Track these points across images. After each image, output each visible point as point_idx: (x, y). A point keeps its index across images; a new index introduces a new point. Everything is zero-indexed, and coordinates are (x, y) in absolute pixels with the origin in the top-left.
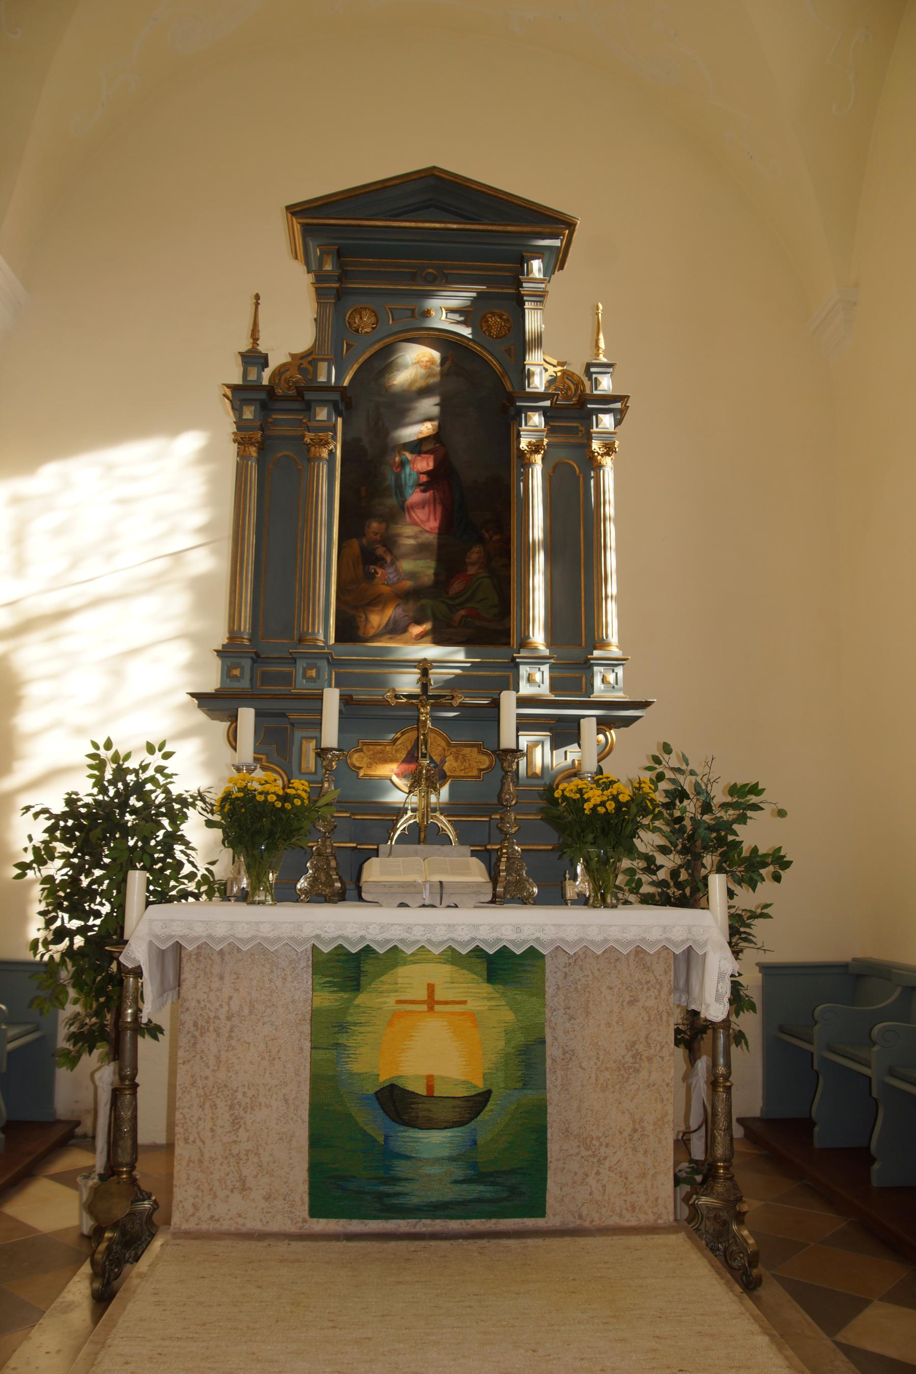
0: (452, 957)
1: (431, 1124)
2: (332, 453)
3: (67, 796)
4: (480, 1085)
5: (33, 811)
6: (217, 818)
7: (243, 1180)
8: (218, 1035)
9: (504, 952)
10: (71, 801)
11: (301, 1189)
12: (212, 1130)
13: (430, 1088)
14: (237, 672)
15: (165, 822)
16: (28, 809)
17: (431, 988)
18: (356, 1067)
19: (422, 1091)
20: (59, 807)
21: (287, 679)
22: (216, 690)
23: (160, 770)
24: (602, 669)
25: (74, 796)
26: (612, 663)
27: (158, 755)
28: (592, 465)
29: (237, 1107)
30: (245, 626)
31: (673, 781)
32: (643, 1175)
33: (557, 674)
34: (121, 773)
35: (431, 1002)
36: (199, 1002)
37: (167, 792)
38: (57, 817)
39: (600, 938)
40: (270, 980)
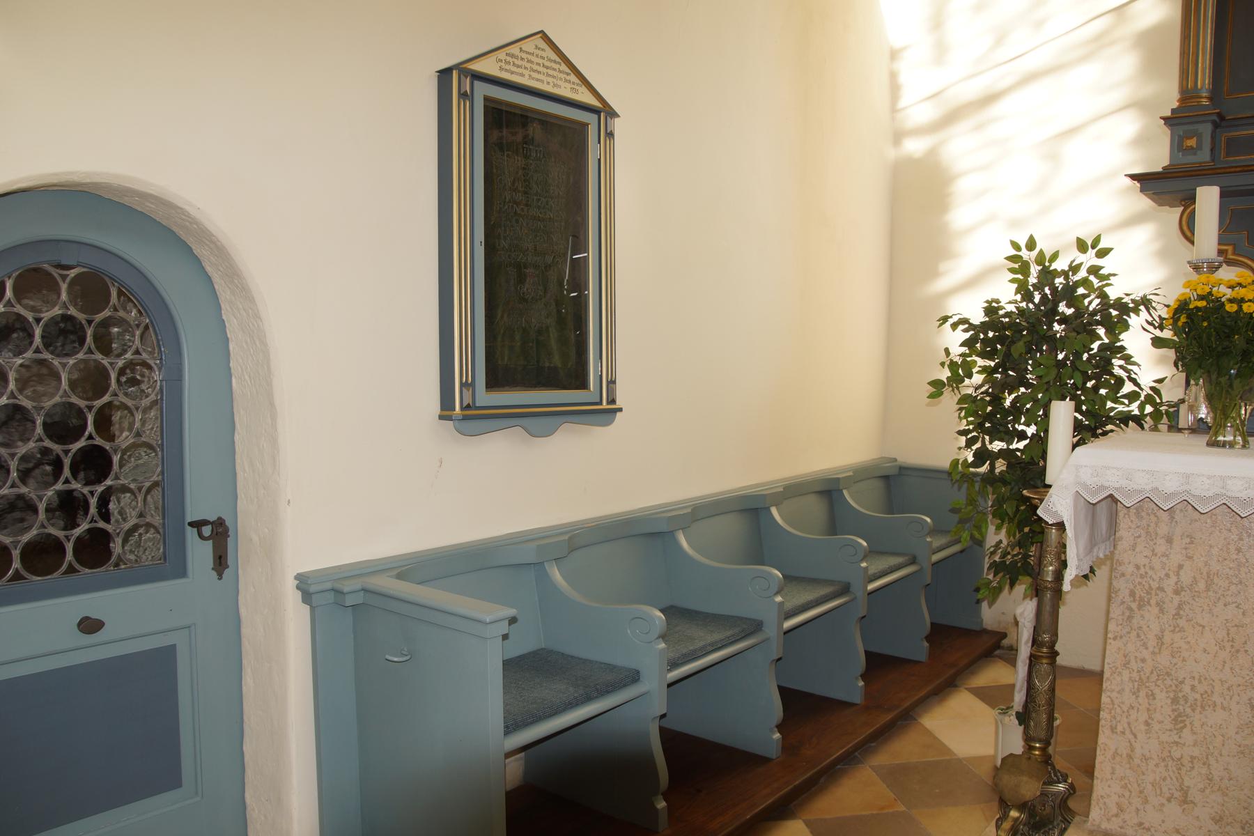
3: (986, 305)
5: (951, 321)
6: (1167, 334)
7: (1185, 791)
8: (1162, 611)
12: (1147, 723)
14: (1192, 142)
15: (1101, 331)
16: (945, 319)
20: (978, 317)
22: (1164, 168)
23: (1094, 270)
25: (994, 304)
27: (1091, 253)
29: (1182, 702)
34: (1047, 275)
36: (1138, 567)
37: (1103, 296)
40: (1239, 550)
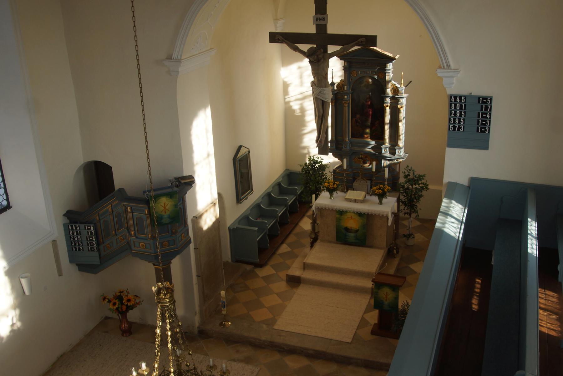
0: (354, 212)
1: (351, 232)
2: (349, 104)
4: (358, 229)
9: (361, 213)
17: (351, 216)
19: (350, 228)
24: (398, 150)
30: (334, 138)
31: (408, 172)
35: (351, 218)
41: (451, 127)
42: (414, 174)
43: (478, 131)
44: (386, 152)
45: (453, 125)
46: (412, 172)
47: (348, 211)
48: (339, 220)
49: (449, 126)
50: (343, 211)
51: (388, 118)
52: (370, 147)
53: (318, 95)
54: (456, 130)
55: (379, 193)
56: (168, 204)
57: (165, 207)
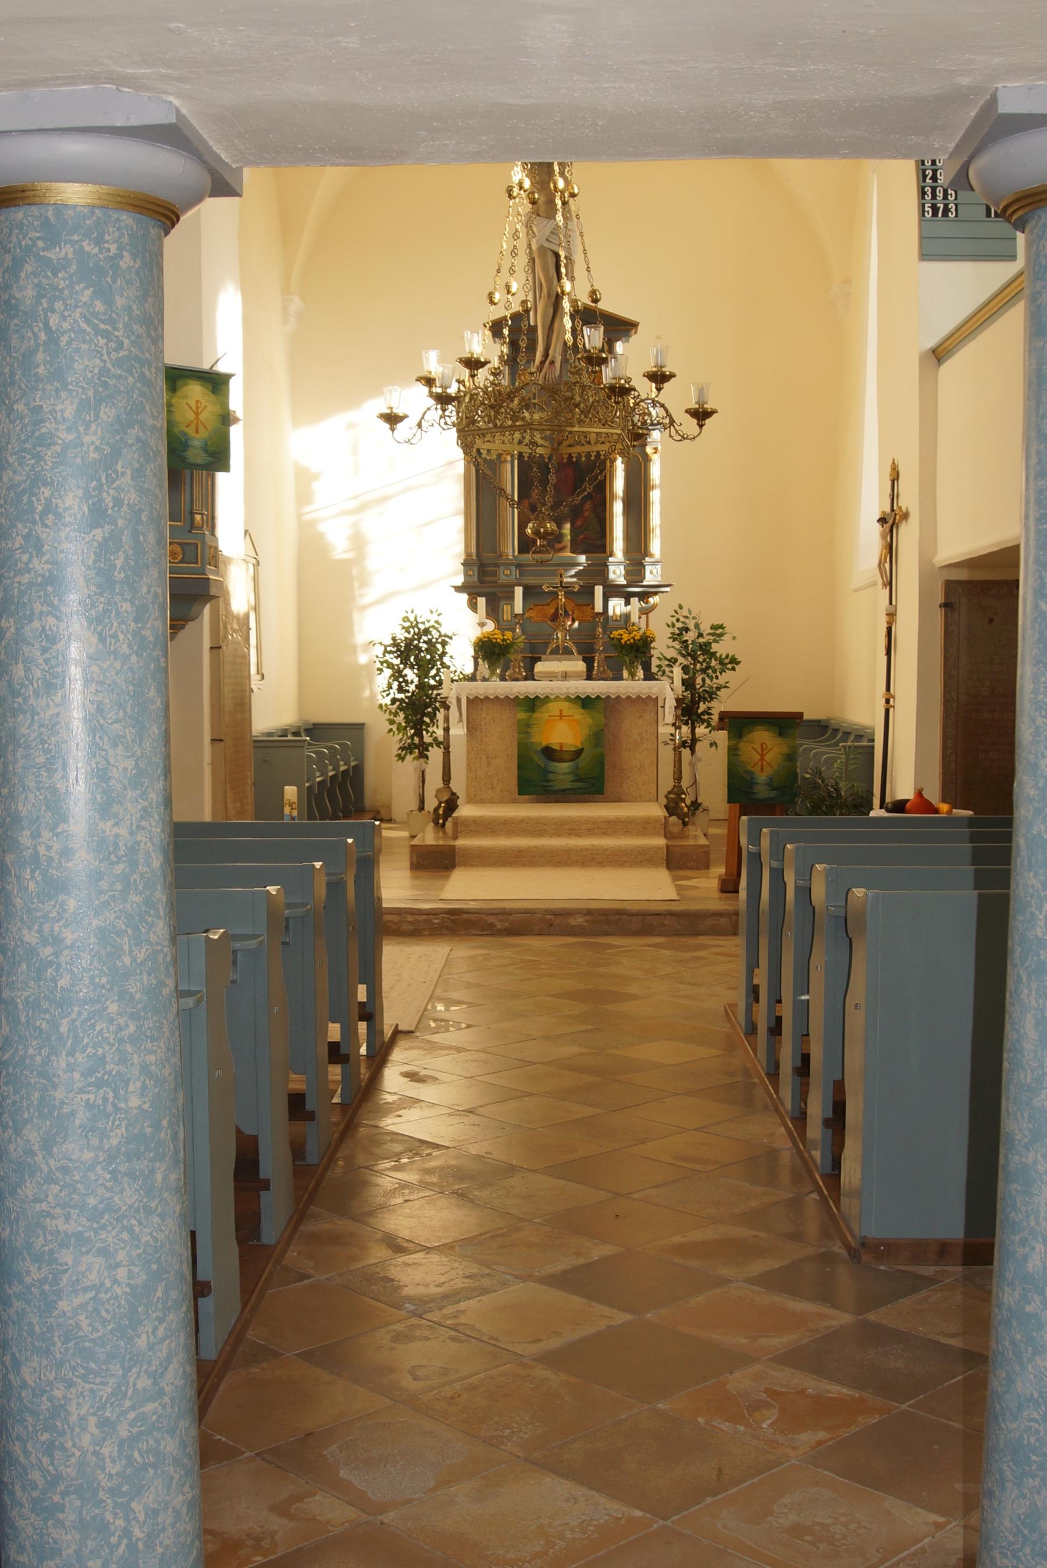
0: (568, 699)
1: (561, 760)
4: (580, 746)
7: (492, 785)
10: (394, 639)
11: (514, 781)
13: (561, 747)
15: (439, 646)
17: (561, 711)
18: (534, 740)
19: (557, 748)
21: (494, 574)
26: (654, 563)
27: (435, 615)
28: (647, 459)
30: (474, 550)
31: (683, 623)
32: (644, 784)
33: (628, 568)
35: (561, 716)
38: (386, 647)
39: (624, 692)
41: (926, 209)
42: (697, 626)
43: (988, 214)
44: (617, 574)
45: (932, 204)
46: (691, 626)
47: (552, 697)
48: (525, 728)
49: (923, 205)
50: (537, 697)
51: (619, 485)
52: (573, 572)
53: (547, 240)
54: (940, 215)
55: (632, 641)
56: (206, 406)
57: (197, 414)
